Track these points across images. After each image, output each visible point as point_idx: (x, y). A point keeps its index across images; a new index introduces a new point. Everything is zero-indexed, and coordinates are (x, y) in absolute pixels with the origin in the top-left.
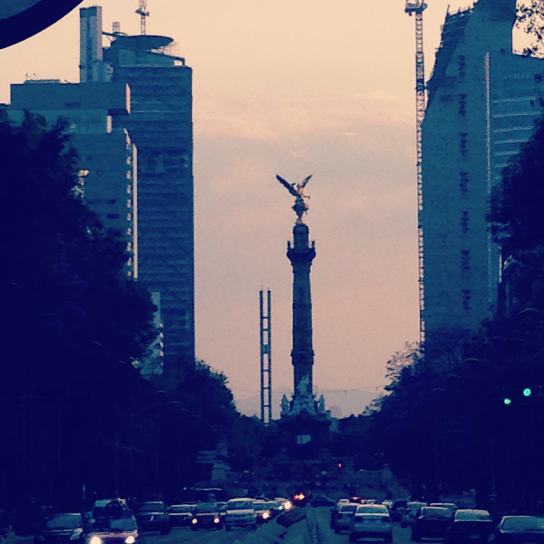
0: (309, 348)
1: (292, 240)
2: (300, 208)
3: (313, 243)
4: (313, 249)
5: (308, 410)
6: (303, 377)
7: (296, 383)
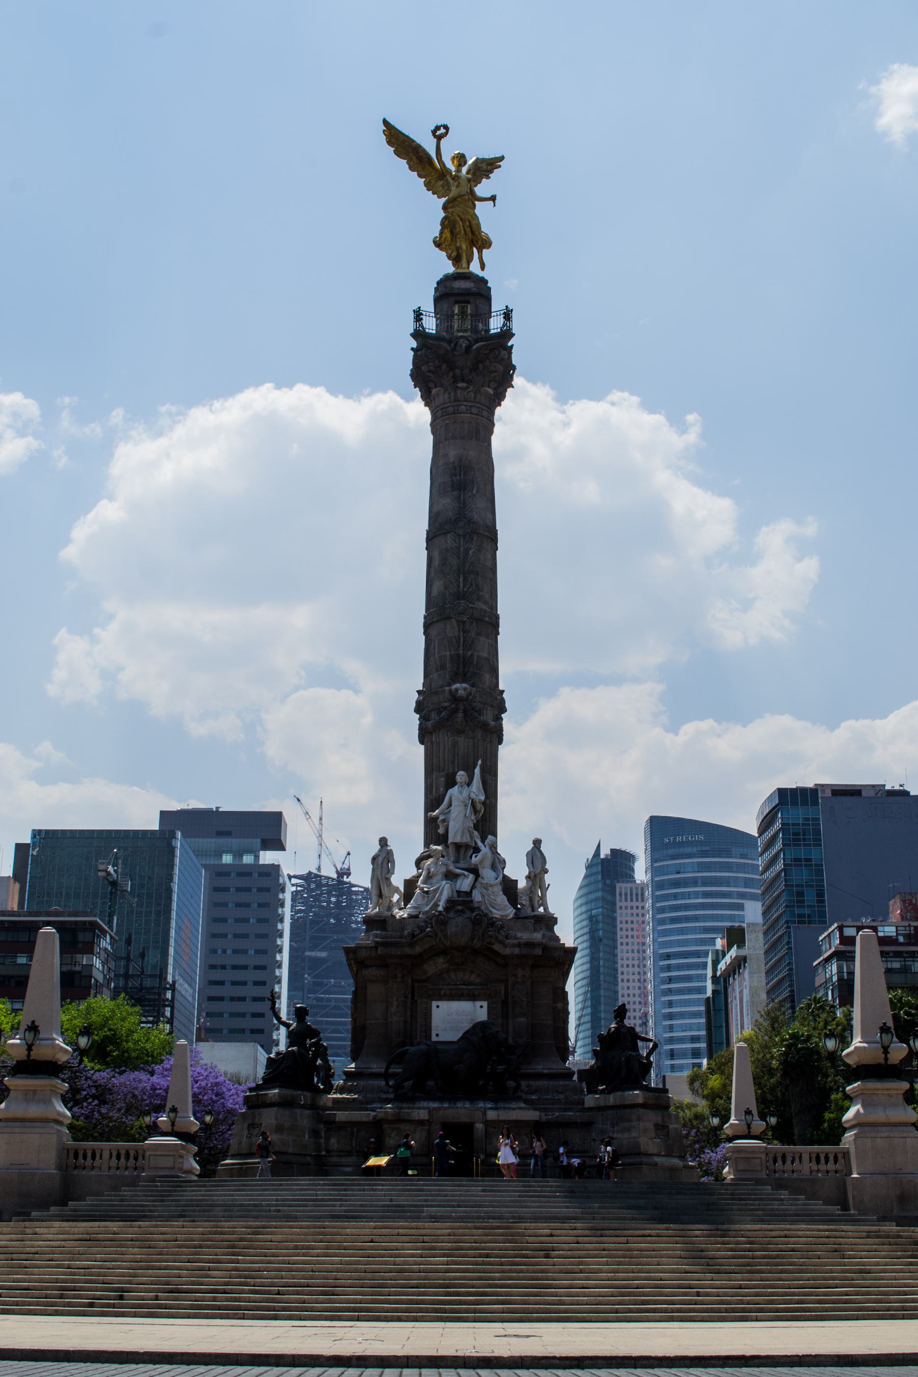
0: (487, 677)
1: (428, 306)
2: (461, 234)
3: (508, 315)
4: (507, 333)
5: (477, 896)
6: (461, 776)
7: (433, 800)
